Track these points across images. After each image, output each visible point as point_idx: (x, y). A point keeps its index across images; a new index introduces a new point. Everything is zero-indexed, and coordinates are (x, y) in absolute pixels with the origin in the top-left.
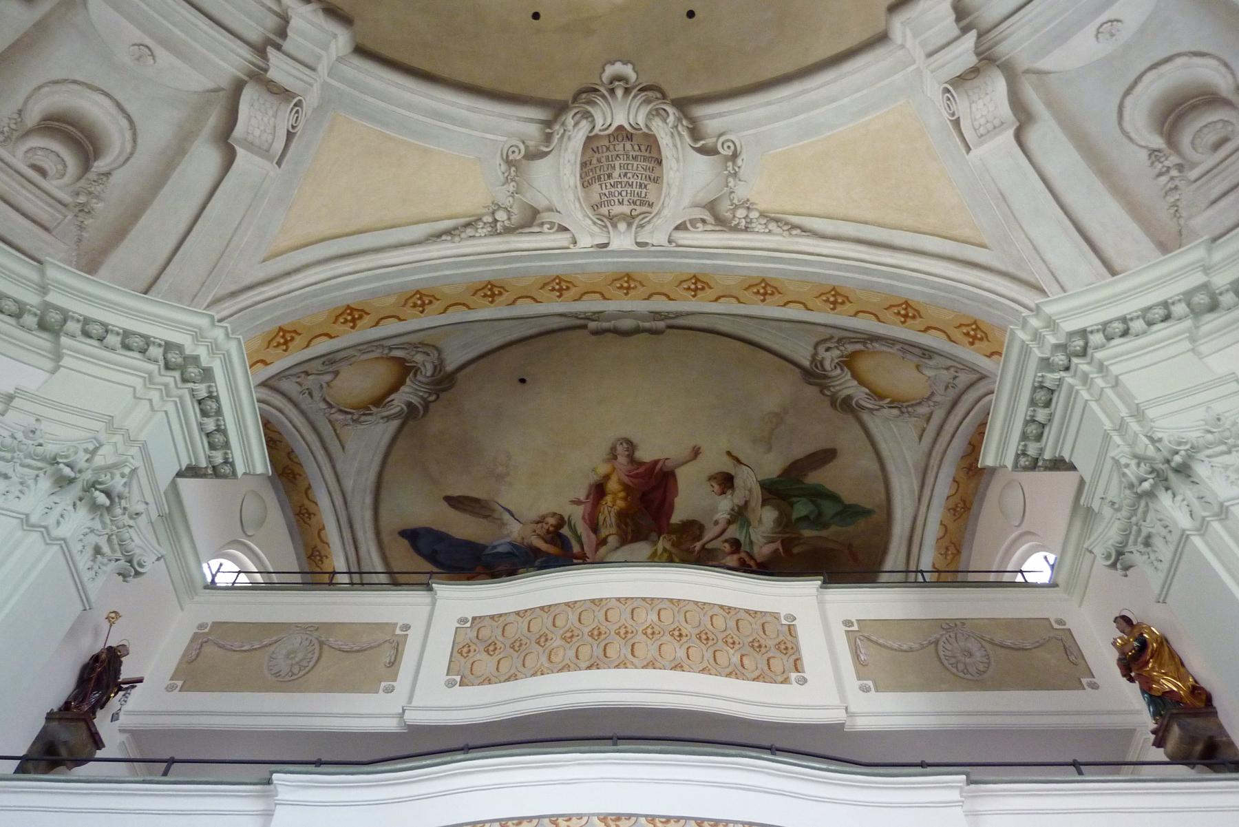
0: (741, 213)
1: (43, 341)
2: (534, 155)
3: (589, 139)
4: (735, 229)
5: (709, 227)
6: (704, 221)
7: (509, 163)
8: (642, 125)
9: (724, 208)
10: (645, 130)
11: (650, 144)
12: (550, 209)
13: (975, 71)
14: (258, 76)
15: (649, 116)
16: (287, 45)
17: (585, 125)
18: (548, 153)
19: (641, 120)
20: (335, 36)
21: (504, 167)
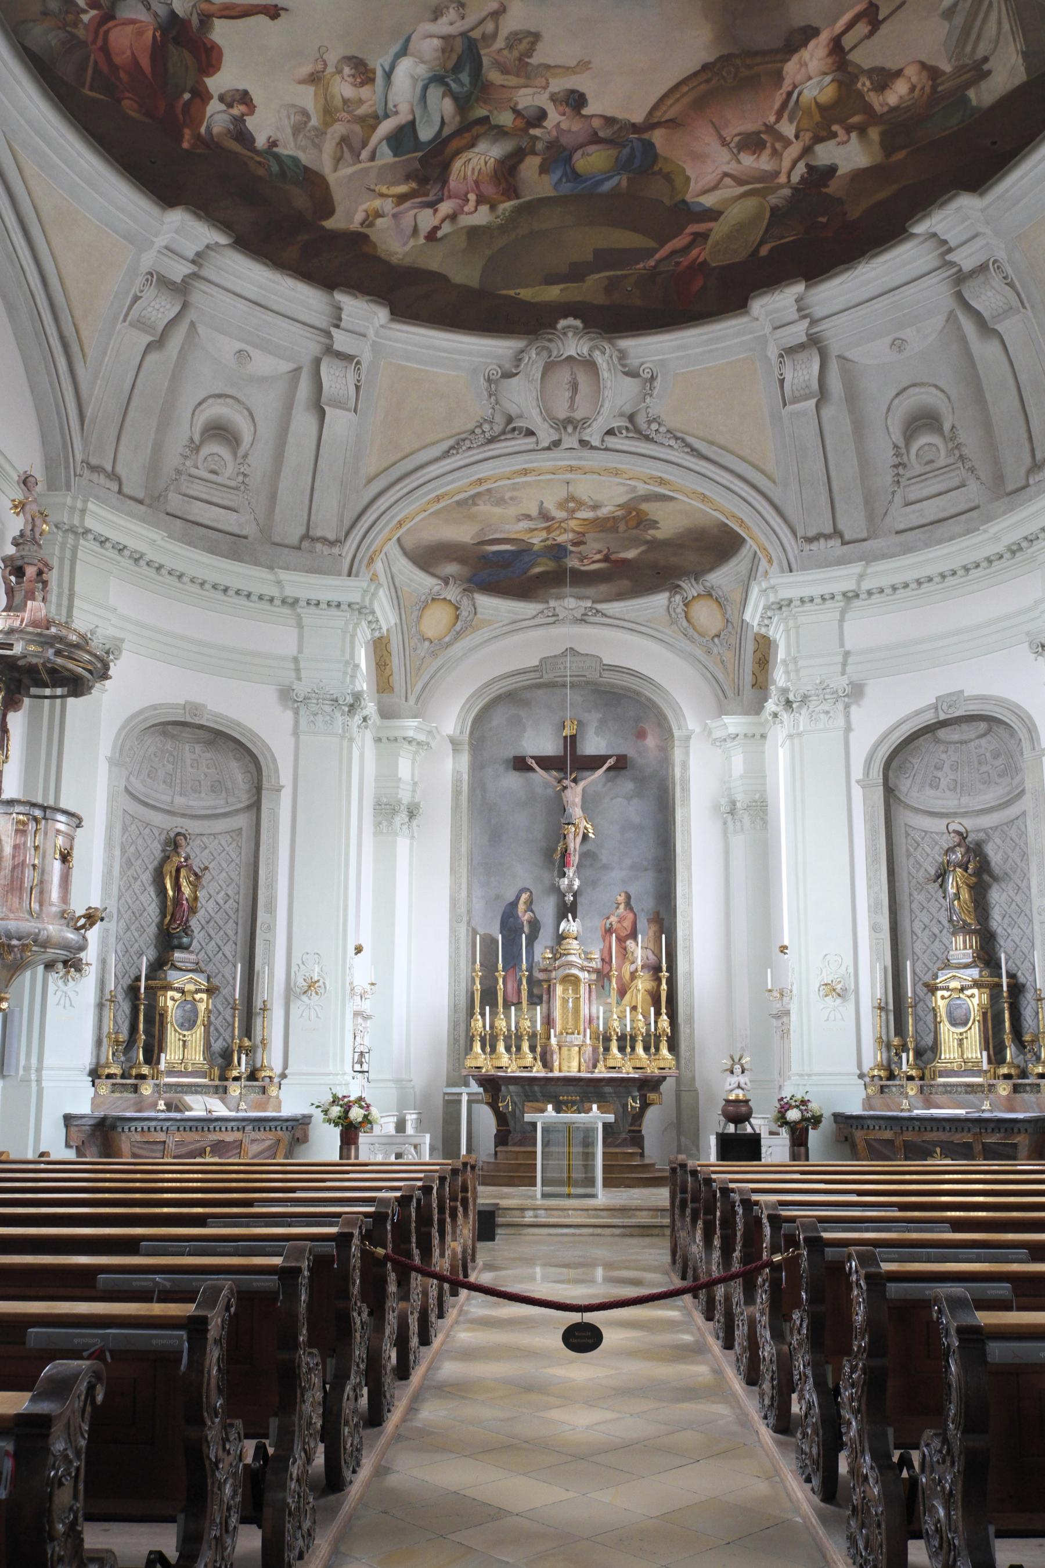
0: (654, 426)
1: (286, 610)
2: (508, 375)
4: (647, 438)
5: (630, 435)
6: (627, 428)
7: (489, 380)
8: (586, 354)
9: (641, 420)
11: (590, 365)
12: (521, 416)
13: (802, 346)
14: (329, 351)
15: (591, 350)
16: (343, 324)
17: (545, 354)
18: (517, 374)
19: (585, 351)
20: (375, 313)
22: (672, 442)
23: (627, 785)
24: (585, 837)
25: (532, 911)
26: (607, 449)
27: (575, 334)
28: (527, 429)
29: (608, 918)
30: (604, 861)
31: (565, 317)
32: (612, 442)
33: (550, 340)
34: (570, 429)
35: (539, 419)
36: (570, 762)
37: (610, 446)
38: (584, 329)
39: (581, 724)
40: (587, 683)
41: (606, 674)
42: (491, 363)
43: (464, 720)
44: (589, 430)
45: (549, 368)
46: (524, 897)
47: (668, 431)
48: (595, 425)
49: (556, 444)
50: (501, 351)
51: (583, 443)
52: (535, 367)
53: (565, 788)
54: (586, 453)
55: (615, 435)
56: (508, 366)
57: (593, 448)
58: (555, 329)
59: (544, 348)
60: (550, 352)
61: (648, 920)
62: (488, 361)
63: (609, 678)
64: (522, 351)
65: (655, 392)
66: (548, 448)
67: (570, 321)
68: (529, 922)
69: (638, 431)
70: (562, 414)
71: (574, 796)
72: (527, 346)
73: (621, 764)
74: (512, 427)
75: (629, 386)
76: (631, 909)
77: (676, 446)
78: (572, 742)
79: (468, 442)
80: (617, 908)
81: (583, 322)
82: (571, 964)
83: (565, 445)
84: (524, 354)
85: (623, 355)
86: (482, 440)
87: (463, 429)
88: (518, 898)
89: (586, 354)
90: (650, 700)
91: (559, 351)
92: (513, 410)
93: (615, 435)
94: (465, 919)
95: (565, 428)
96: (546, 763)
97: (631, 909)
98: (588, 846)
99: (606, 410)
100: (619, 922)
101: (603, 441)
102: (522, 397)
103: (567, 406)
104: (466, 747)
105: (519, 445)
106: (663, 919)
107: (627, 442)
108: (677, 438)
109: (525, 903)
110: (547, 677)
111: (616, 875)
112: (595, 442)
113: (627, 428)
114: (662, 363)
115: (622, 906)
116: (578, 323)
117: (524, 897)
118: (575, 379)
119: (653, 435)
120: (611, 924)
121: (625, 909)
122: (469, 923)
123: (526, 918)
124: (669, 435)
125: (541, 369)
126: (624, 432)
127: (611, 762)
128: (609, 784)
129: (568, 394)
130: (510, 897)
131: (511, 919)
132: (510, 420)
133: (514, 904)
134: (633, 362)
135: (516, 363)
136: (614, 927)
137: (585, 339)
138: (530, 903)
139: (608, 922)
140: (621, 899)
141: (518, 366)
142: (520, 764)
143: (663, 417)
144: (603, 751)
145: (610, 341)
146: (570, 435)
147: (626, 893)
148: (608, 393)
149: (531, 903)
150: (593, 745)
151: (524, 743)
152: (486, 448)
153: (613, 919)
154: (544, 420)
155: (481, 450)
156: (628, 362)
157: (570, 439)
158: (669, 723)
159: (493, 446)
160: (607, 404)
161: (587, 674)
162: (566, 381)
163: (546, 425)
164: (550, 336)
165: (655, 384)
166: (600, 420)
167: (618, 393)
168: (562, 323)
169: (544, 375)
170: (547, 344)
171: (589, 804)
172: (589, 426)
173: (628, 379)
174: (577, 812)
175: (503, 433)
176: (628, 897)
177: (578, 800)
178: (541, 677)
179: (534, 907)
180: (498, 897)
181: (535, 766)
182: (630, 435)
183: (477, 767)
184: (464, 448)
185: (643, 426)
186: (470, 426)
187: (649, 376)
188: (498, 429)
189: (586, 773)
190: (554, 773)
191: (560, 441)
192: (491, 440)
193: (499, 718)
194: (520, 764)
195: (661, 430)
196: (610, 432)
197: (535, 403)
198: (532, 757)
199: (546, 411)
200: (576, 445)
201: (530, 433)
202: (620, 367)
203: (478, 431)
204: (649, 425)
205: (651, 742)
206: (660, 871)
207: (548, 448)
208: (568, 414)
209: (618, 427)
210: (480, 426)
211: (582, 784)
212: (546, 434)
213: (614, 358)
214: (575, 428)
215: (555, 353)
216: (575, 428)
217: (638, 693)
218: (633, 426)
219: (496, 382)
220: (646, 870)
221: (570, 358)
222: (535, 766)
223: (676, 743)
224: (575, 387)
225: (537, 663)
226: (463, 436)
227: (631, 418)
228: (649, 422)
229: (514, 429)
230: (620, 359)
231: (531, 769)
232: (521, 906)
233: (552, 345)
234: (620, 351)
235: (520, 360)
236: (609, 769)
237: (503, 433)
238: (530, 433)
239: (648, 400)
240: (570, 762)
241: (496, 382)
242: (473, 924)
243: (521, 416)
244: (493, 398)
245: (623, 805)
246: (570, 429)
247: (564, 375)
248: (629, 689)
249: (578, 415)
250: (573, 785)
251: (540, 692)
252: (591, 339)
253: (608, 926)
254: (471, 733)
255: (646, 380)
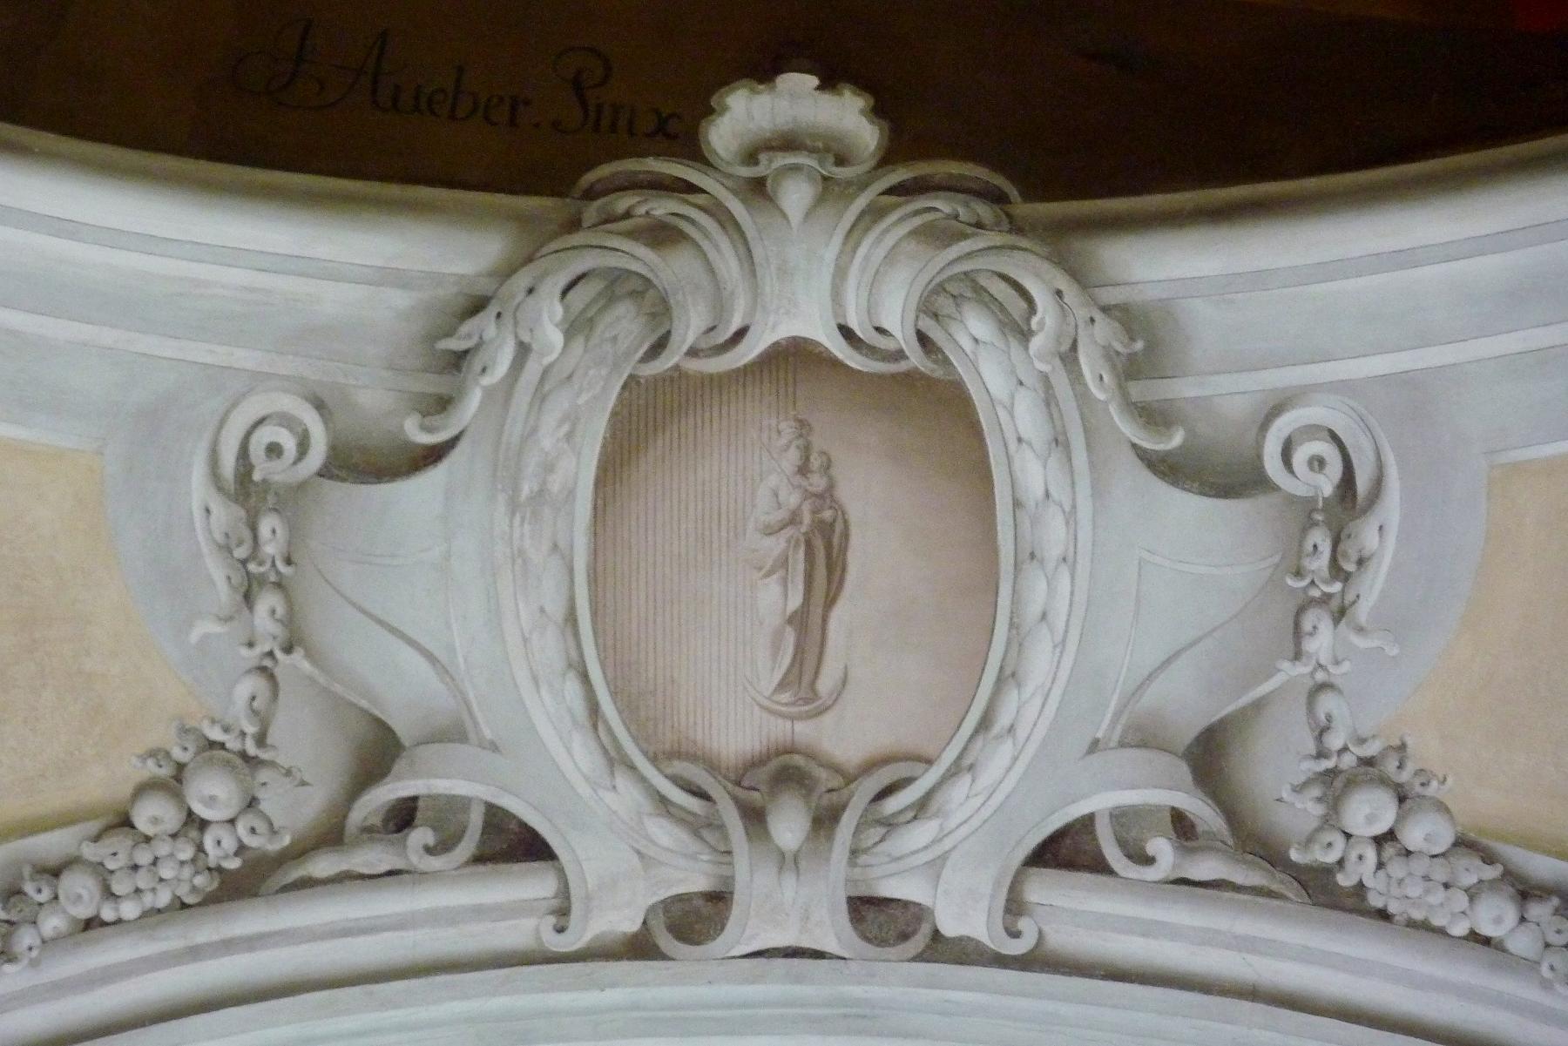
0: (1369, 811)
2: (372, 462)
3: (631, 377)
4: (1323, 891)
5: (1206, 868)
6: (1182, 826)
7: (245, 489)
8: (902, 337)
9: (1277, 776)
10: (916, 359)
11: (929, 405)
12: (453, 733)
15: (934, 303)
17: (625, 326)
18: (434, 455)
21: (225, 515)
22: (1495, 916)
26: (1038, 961)
27: (830, 191)
28: (496, 818)
31: (764, 71)
32: (1071, 910)
33: (662, 235)
34: (789, 825)
35: (577, 757)
37: (1066, 938)
38: (888, 157)
42: (257, 380)
44: (918, 835)
45: (647, 420)
47: (1463, 844)
48: (963, 802)
49: (695, 919)
50: (333, 300)
51: (876, 916)
52: (560, 403)
54: (897, 982)
55: (1100, 867)
56: (380, 404)
57: (943, 949)
58: (695, 152)
59: (622, 286)
60: (660, 311)
62: (244, 358)
64: (476, 306)
65: (1370, 591)
66: (639, 948)
67: (795, 101)
69: (1256, 843)
70: (738, 726)
72: (506, 272)
74: (389, 801)
75: (1199, 550)
77: (1522, 943)
79: (80, 894)
81: (878, 111)
83: (750, 927)
84: (484, 324)
85: (1146, 345)
86: (177, 875)
87: (52, 799)
89: (902, 337)
91: (720, 306)
92: (402, 689)
93: (1100, 867)
95: (755, 817)
99: (1030, 709)
101: (1015, 906)
102: (461, 600)
103: (768, 672)
105: (437, 918)
107: (1184, 914)
108: (1526, 891)
112: (965, 912)
113: (1182, 826)
114: (1412, 399)
116: (847, 116)
118: (826, 497)
119: (1362, 868)
124: (1471, 871)
125: (596, 430)
126: (1161, 847)
129: (775, 599)
132: (378, 751)
134: (1217, 391)
135: (433, 384)
137: (896, 227)
141: (443, 404)
143: (1427, 749)
145: (1058, 241)
146: (787, 862)
148: (1046, 593)
152: (208, 929)
154: (616, 760)
155: (172, 938)
156: (1183, 389)
157: (790, 889)
159: (249, 920)
160: (1040, 662)
162: (764, 510)
163: (625, 797)
164: (663, 207)
165: (1367, 535)
166: (997, 761)
167: (1119, 599)
168: (743, 115)
169: (615, 466)
170: (640, 258)
172: (921, 808)
173: (1186, 509)
175: (331, 836)
182: (1206, 868)
184: (52, 923)
185: (1292, 811)
186: (104, 780)
187: (1327, 484)
188: (292, 808)
191: (719, 899)
192: (242, 884)
195: (1413, 836)
196: (1066, 851)
197: (550, 648)
199: (629, 711)
200: (830, 929)
201: (516, 844)
202: (1129, 429)
203: (153, 814)
204: (1334, 804)
207: (639, 948)
208: (779, 730)
209: (1120, 816)
210: (174, 783)
212: (621, 858)
213: (1088, 363)
214: (825, 821)
215: (690, 326)
216: (825, 821)
218: (1219, 805)
219: (290, 500)
221: (794, 358)
224: (824, 551)
226: (51, 845)
227: (1209, 756)
228: (1334, 786)
229: (403, 816)
230: (1130, 370)
233: (670, 268)
234: (1127, 317)
235: (458, 360)
237: (331, 836)
238: (516, 844)
239: (1322, 640)
241: (290, 500)
243: (453, 733)
244: (268, 601)
246: (789, 825)
247: (749, 472)
249: (844, 737)
252: (937, 235)
255: (1305, 512)
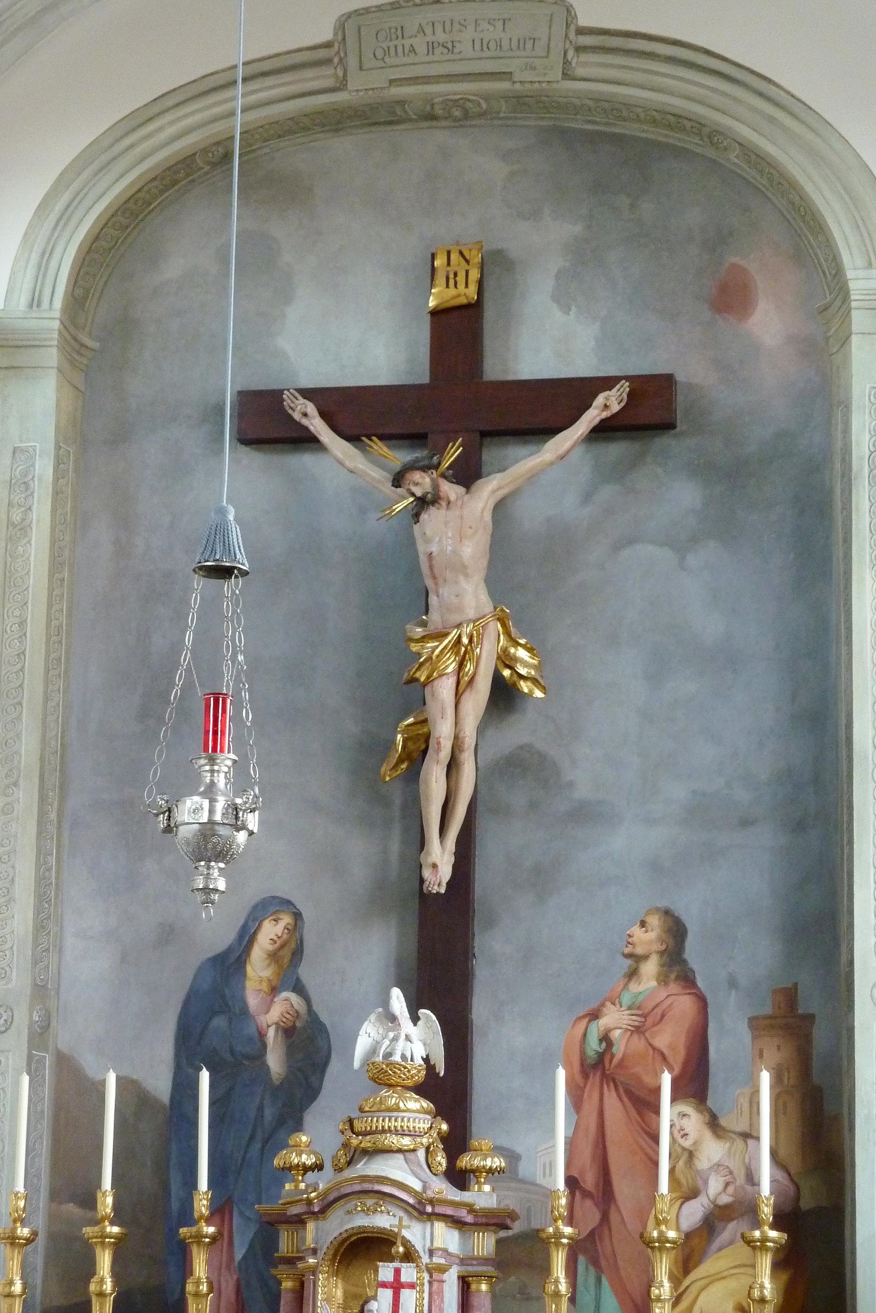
23: (671, 492)
24: (504, 695)
25: (299, 988)
29: (594, 1015)
30: (583, 790)
36: (456, 407)
39: (495, 265)
40: (520, 102)
41: (588, 65)
43: (46, 255)
46: (270, 932)
53: (423, 503)
61: (755, 1023)
63: (601, 78)
68: (288, 1032)
71: (459, 531)
73: (648, 413)
76: (687, 980)
78: (458, 331)
80: (633, 974)
82: (375, 1193)
88: (246, 938)
90: (754, 156)
94: (23, 1018)
96: (357, 412)
97: (687, 980)
98: (516, 733)
100: (638, 1030)
104: (52, 356)
106: (810, 1018)
109: (273, 956)
110: (364, 85)
111: (629, 841)
115: (650, 968)
117: (270, 932)
120: (606, 1038)
121: (663, 979)
122: (40, 1036)
123: (275, 1014)
127: (608, 403)
128: (608, 492)
130: (215, 931)
131: (219, 1022)
133: (230, 963)
136: (619, 1050)
138: (291, 955)
139: (595, 1030)
140: (648, 938)
142: (267, 424)
144: (583, 366)
147: (667, 913)
149: (298, 953)
150: (544, 339)
151: (285, 343)
153: (615, 1019)
158: (829, 244)
161: (512, 65)
171: (519, 569)
174: (466, 597)
176: (676, 931)
177: (473, 550)
178: (341, 86)
179: (305, 972)
180: (168, 935)
181: (318, 426)
183: (98, 433)
189: (514, 450)
190: (379, 447)
193: (196, 249)
194: (267, 424)
198: (308, 394)
205: (769, 323)
206: (799, 827)
211: (489, 489)
217: (714, 136)
220: (746, 823)
222: (318, 426)
223: (859, 320)
225: (327, 35)
231: (306, 440)
232: (258, 969)
236: (603, 431)
240: (456, 407)
242: (64, 1037)
245: (661, 566)
248: (678, 121)
250: (451, 490)
251: (343, 146)
253: (594, 1045)
254: (78, 301)
